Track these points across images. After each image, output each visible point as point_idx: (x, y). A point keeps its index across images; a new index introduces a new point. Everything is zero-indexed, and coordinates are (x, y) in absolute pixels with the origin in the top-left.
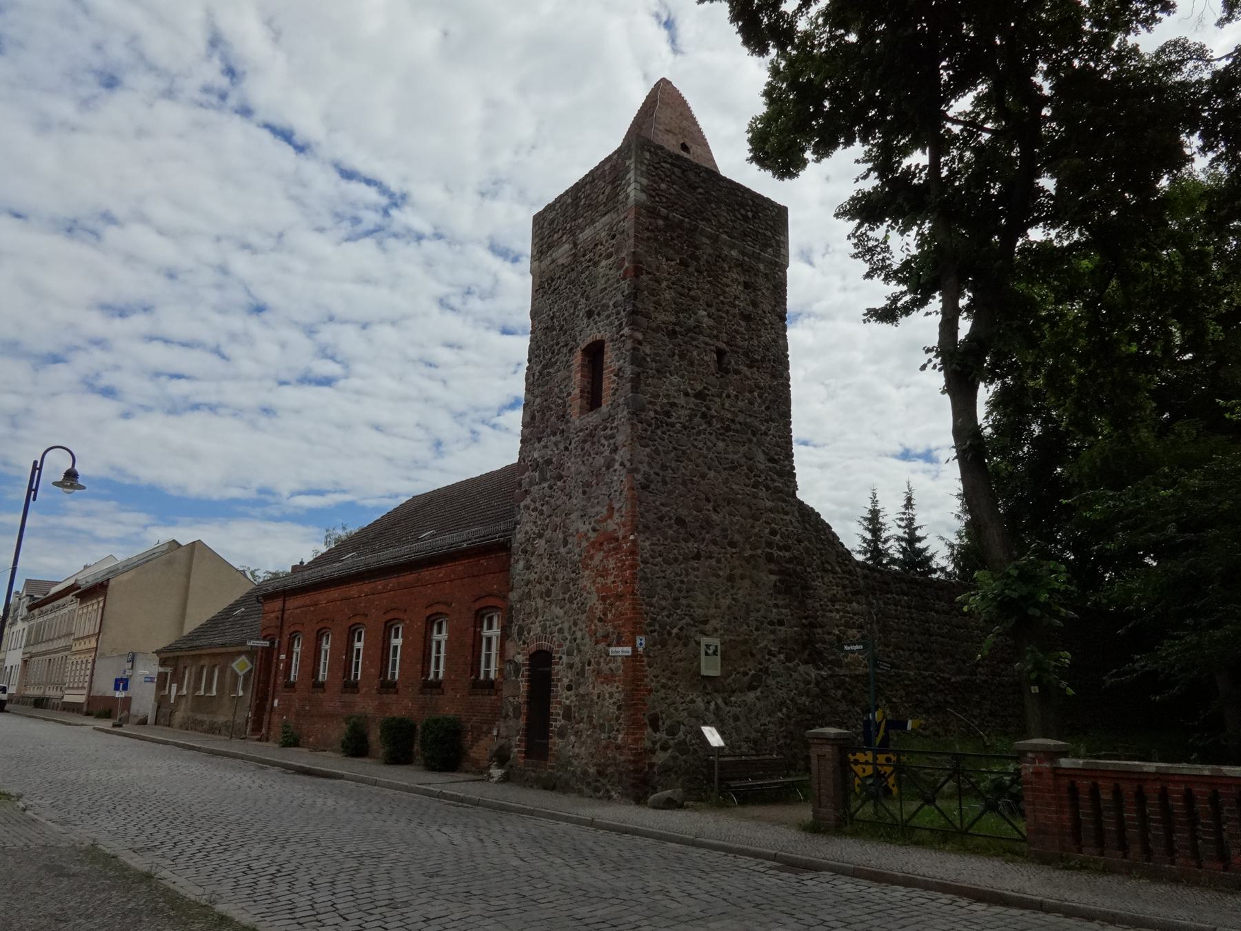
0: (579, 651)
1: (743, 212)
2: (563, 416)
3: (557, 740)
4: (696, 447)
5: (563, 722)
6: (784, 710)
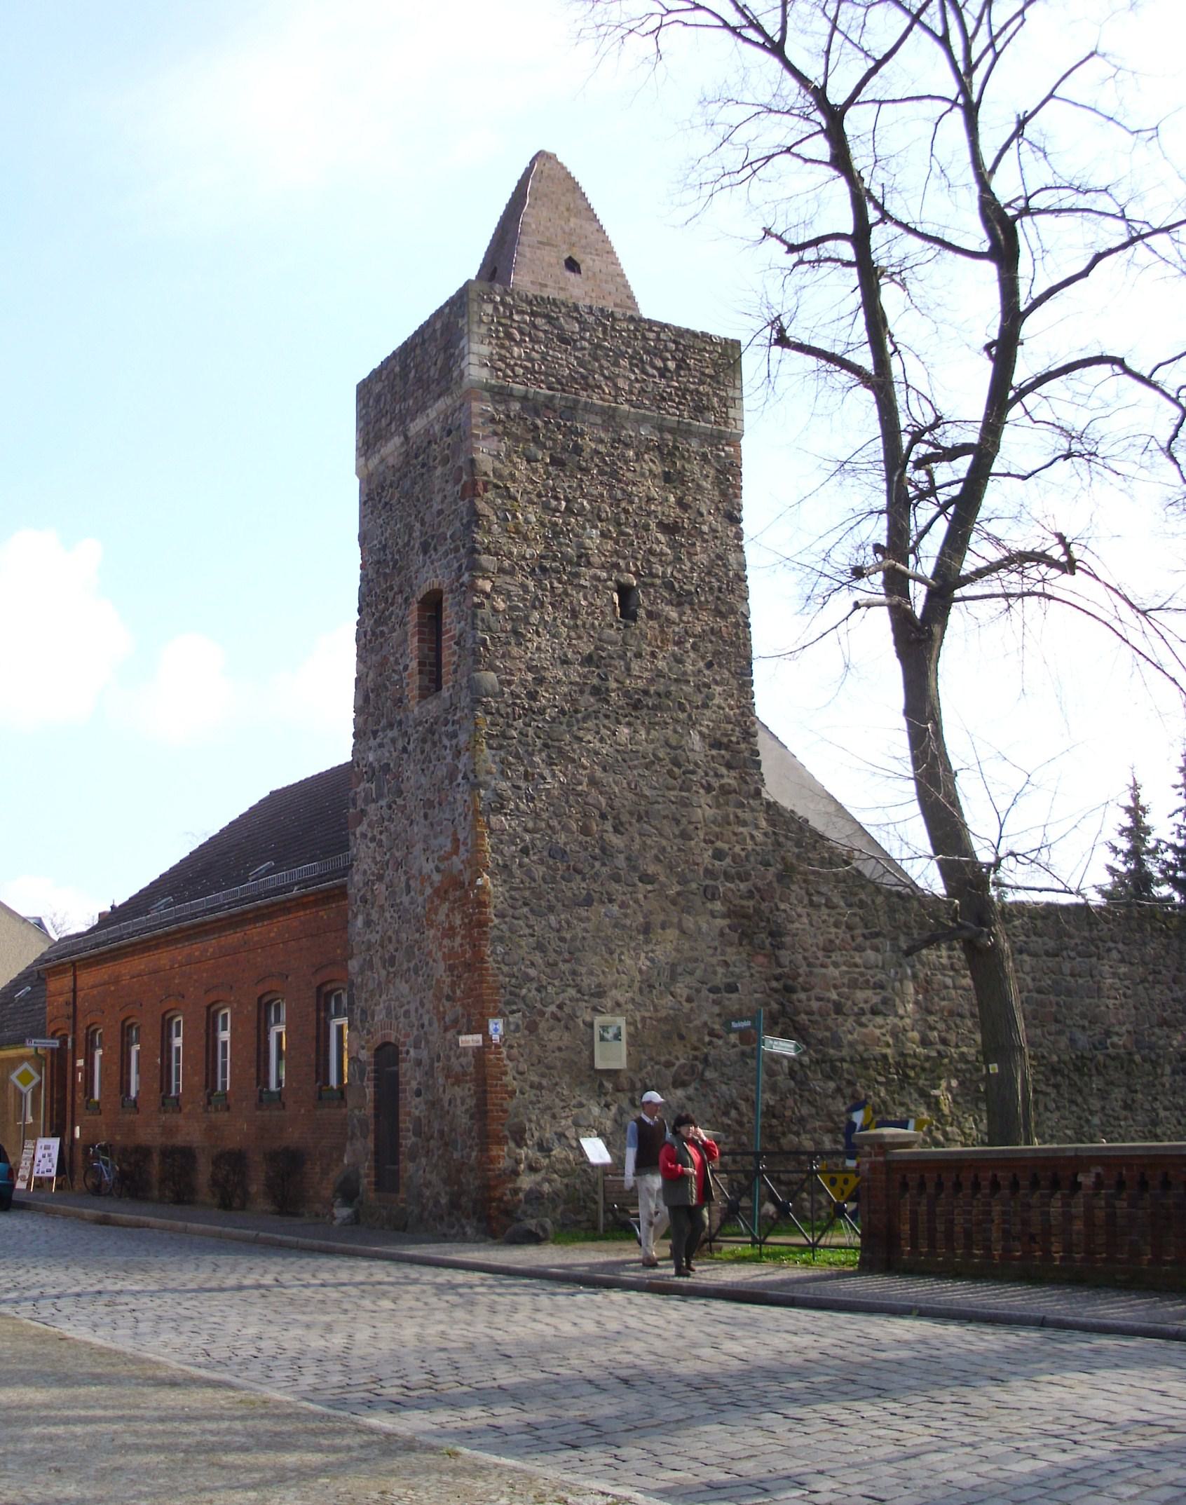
0: (427, 1042)
1: (659, 363)
2: (400, 700)
3: (411, 1166)
4: (580, 739)
5: (413, 1139)
6: (733, 1113)
